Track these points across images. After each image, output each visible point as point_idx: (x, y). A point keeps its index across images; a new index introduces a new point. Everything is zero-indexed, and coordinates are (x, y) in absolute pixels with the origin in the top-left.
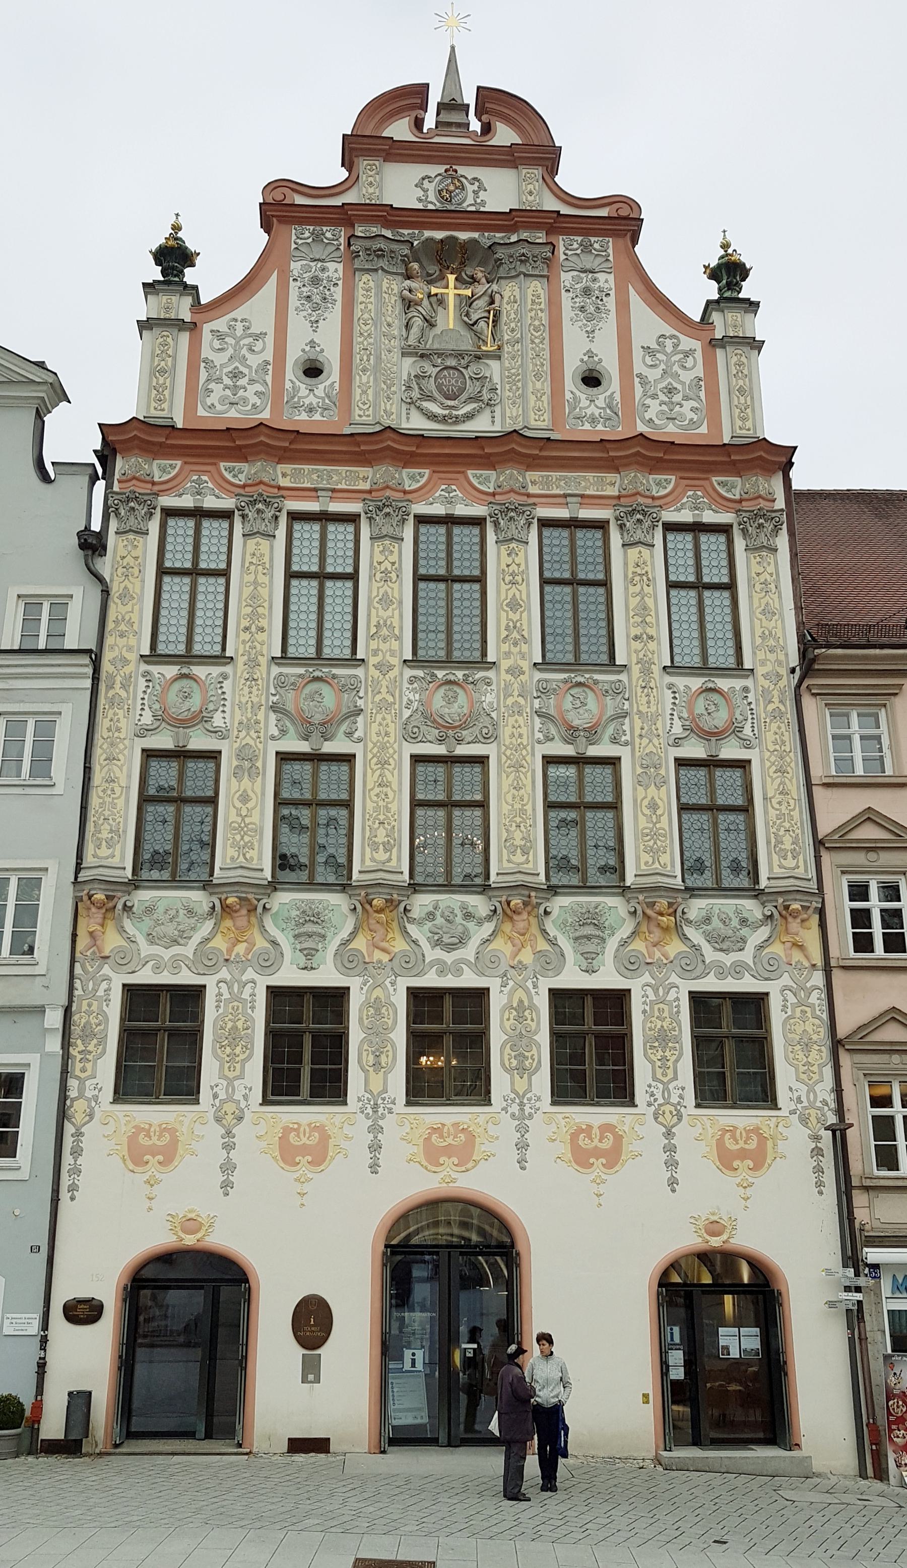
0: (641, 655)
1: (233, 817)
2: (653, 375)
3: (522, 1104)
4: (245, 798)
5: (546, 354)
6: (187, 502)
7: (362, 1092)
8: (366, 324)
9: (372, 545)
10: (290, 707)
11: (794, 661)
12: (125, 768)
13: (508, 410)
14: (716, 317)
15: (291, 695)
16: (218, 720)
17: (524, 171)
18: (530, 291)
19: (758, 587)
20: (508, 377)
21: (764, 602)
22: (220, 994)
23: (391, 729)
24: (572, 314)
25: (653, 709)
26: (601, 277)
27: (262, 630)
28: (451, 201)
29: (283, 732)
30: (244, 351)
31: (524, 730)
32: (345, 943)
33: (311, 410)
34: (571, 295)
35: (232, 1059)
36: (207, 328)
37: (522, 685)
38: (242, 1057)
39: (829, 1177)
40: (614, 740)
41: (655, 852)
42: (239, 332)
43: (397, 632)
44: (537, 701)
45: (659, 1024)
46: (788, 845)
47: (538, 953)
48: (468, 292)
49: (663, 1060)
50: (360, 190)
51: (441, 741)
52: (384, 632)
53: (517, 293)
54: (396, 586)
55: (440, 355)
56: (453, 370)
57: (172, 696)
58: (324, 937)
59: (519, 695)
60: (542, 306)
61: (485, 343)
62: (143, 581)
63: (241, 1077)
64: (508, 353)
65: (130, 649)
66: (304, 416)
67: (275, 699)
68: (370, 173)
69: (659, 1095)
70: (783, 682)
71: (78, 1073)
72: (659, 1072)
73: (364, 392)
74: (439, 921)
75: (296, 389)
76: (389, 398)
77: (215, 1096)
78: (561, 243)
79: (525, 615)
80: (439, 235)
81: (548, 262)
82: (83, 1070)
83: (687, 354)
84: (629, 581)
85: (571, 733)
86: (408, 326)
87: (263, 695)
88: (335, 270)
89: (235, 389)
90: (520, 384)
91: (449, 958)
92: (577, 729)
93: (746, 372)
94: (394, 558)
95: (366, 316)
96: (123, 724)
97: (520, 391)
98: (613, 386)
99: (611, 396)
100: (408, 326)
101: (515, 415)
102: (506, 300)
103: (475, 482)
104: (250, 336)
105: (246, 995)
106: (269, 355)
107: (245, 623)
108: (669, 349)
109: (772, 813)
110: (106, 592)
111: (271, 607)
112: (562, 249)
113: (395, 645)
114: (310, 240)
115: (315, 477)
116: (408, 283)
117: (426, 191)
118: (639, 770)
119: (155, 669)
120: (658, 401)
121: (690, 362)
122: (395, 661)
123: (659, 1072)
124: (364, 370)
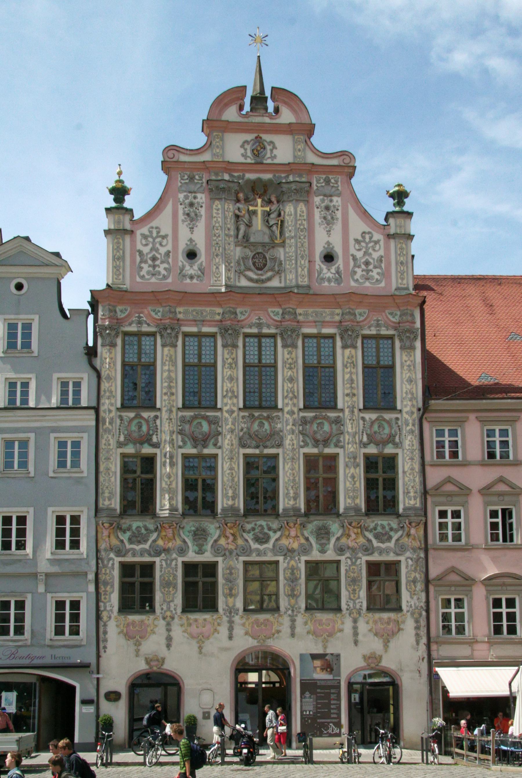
0: (349, 404)
1: (164, 485)
3: (293, 611)
5: (306, 245)
6: (133, 328)
7: (224, 607)
8: (217, 229)
9: (223, 350)
11: (420, 405)
12: (114, 463)
14: (391, 221)
15: (187, 427)
16: (155, 439)
17: (296, 137)
18: (298, 209)
19: (405, 368)
21: (408, 375)
22: (161, 565)
23: (234, 442)
24: (320, 221)
26: (335, 199)
27: (172, 394)
30: (158, 245)
31: (295, 442)
32: (216, 541)
33: (192, 277)
34: (319, 210)
36: (138, 233)
37: (294, 420)
38: (172, 592)
39: (424, 640)
40: (336, 446)
41: (354, 498)
42: (155, 235)
43: (236, 394)
45: (352, 575)
46: (412, 494)
47: (301, 545)
48: (268, 209)
50: (212, 151)
51: (257, 447)
52: (230, 394)
54: (235, 371)
55: (254, 246)
57: (134, 428)
58: (206, 539)
59: (293, 425)
61: (276, 239)
62: (116, 370)
63: (172, 601)
65: (112, 405)
66: (188, 281)
67: (180, 428)
68: (217, 140)
69: (351, 605)
70: (415, 415)
71: (103, 599)
74: (257, 531)
75: (184, 266)
77: (162, 609)
78: (315, 179)
81: (308, 192)
82: (105, 598)
83: (377, 242)
84: (345, 366)
85: (316, 443)
86: (238, 229)
88: (201, 198)
89: (154, 266)
90: (293, 262)
91: (262, 547)
92: (318, 441)
93: (404, 253)
94: (234, 356)
96: (111, 442)
97: (294, 266)
98: (340, 262)
99: (338, 268)
100: (238, 229)
103: (272, 315)
104: (160, 236)
106: (169, 247)
107: (165, 391)
108: (367, 240)
109: (407, 479)
110: (99, 376)
111: (176, 383)
113: (235, 401)
114: (187, 181)
115: (194, 313)
116: (238, 205)
117: (246, 150)
118: (347, 460)
119: (124, 414)
120: (361, 269)
122: (235, 409)
123: (352, 596)
124: (217, 255)
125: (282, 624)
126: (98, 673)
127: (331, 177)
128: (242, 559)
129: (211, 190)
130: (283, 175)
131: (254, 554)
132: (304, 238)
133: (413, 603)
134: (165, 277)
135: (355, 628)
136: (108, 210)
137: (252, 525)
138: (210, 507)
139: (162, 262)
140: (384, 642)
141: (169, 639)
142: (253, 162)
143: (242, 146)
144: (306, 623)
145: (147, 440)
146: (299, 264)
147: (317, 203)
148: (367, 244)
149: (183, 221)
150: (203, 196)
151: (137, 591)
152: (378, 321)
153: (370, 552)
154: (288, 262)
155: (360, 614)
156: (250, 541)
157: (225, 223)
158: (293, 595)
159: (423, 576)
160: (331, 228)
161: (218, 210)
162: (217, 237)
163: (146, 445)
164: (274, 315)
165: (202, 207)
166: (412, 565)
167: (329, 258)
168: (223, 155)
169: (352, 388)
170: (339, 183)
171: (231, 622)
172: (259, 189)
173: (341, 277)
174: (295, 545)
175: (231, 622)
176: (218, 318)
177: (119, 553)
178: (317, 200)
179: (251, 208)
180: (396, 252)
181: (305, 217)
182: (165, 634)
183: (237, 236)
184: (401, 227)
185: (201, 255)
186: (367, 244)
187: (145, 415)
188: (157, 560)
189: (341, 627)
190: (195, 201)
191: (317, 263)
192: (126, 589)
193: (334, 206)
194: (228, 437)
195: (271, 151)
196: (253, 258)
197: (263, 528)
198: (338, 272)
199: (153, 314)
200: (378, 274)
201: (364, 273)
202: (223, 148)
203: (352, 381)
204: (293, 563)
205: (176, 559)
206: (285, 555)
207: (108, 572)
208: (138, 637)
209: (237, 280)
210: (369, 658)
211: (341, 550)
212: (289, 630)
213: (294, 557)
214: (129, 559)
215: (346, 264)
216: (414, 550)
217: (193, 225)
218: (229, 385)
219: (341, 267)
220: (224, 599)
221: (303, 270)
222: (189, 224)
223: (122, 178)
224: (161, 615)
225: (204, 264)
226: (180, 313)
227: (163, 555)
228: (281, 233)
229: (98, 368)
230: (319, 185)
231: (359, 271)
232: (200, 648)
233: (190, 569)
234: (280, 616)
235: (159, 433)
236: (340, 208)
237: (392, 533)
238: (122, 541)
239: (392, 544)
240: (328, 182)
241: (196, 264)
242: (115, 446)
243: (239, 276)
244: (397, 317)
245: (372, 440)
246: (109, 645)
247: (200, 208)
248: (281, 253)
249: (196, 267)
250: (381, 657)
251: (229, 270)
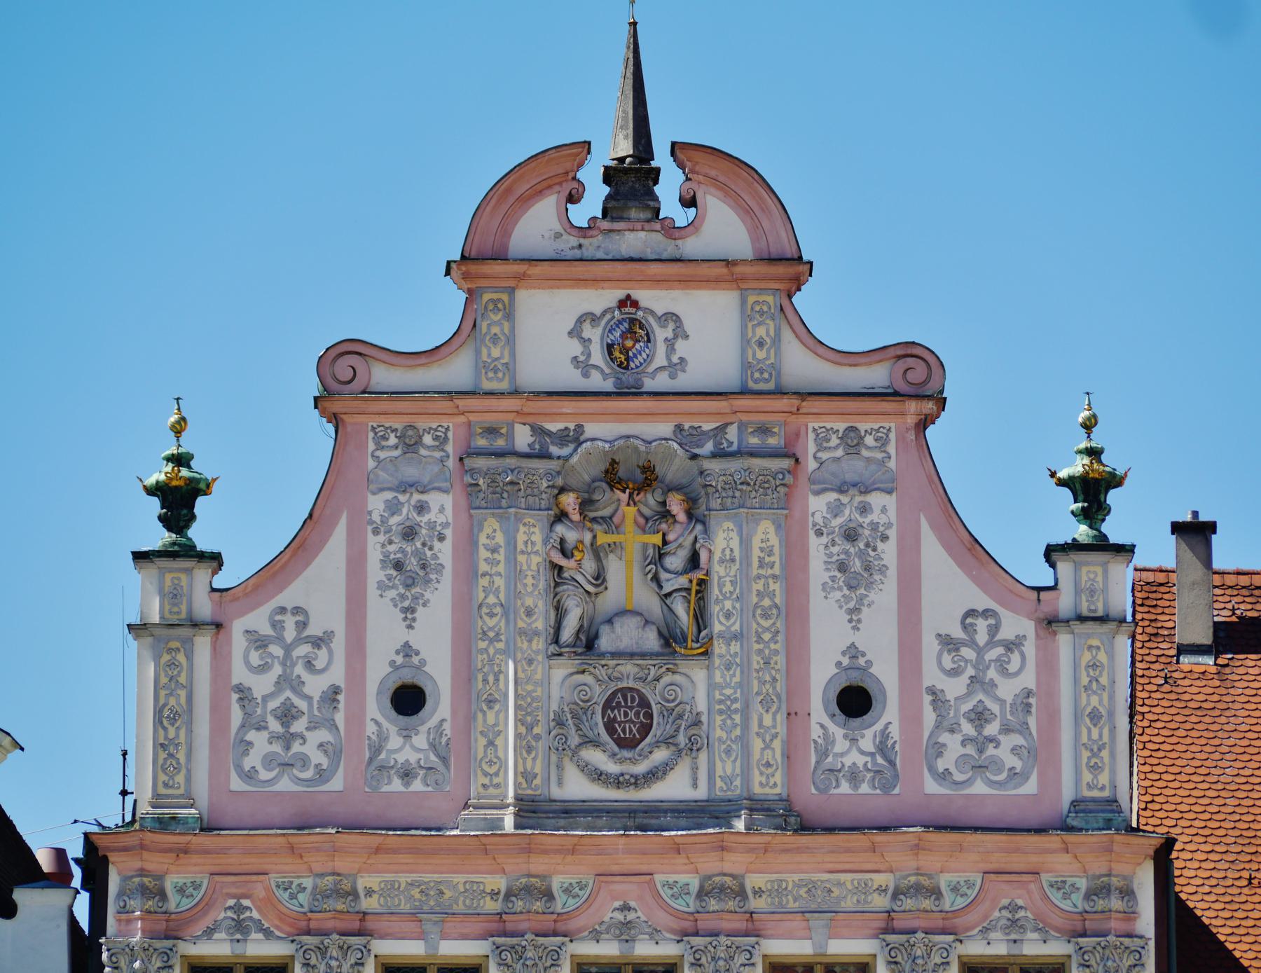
2: (954, 688)
5: (780, 661)
8: (491, 615)
13: (719, 765)
14: (1065, 567)
18: (756, 543)
20: (720, 702)
24: (825, 577)
26: (876, 499)
28: (627, 368)
30: (299, 670)
33: (407, 774)
34: (824, 540)
36: (238, 627)
42: (290, 634)
53: (735, 544)
60: (777, 570)
64: (721, 656)
66: (397, 785)
75: (383, 738)
83: (1010, 646)
88: (443, 507)
89: (287, 739)
90: (737, 718)
93: (1104, 680)
95: (491, 599)
97: (738, 732)
98: (889, 715)
99: (885, 734)
101: (729, 772)
103: (666, 893)
106: (337, 675)
108: (982, 638)
112: (812, 448)
114: (397, 453)
115: (416, 893)
116: (560, 529)
117: (586, 342)
121: (1016, 658)
127: (862, 427)
132: (773, 639)
134: (322, 775)
136: (139, 556)
142: (609, 386)
143: (575, 332)
146: (754, 727)
147: (818, 519)
148: (980, 651)
149: (382, 586)
150: (447, 500)
154: (719, 719)
157: (518, 595)
160: (861, 599)
162: (491, 641)
165: (441, 538)
167: (855, 701)
168: (510, 368)
170: (892, 449)
172: (631, 476)
173: (892, 763)
176: (491, 906)
178: (818, 505)
180: (1076, 680)
181: (777, 570)
184: (1092, 592)
185: (437, 703)
186: (980, 651)
191: (815, 719)
193: (874, 526)
195: (670, 345)
196: (608, 705)
198: (883, 747)
200: (1015, 750)
202: (511, 341)
209: (553, 778)
215: (911, 718)
217: (415, 598)
219: (895, 731)
222: (403, 597)
223: (188, 444)
225: (447, 727)
226: (369, 892)
228: (701, 618)
231: (953, 746)
236: (892, 533)
240: (852, 440)
241: (423, 729)
243: (560, 767)
244: (1078, 898)
247: (437, 545)
248: (696, 684)
249: (420, 741)
251: (529, 749)
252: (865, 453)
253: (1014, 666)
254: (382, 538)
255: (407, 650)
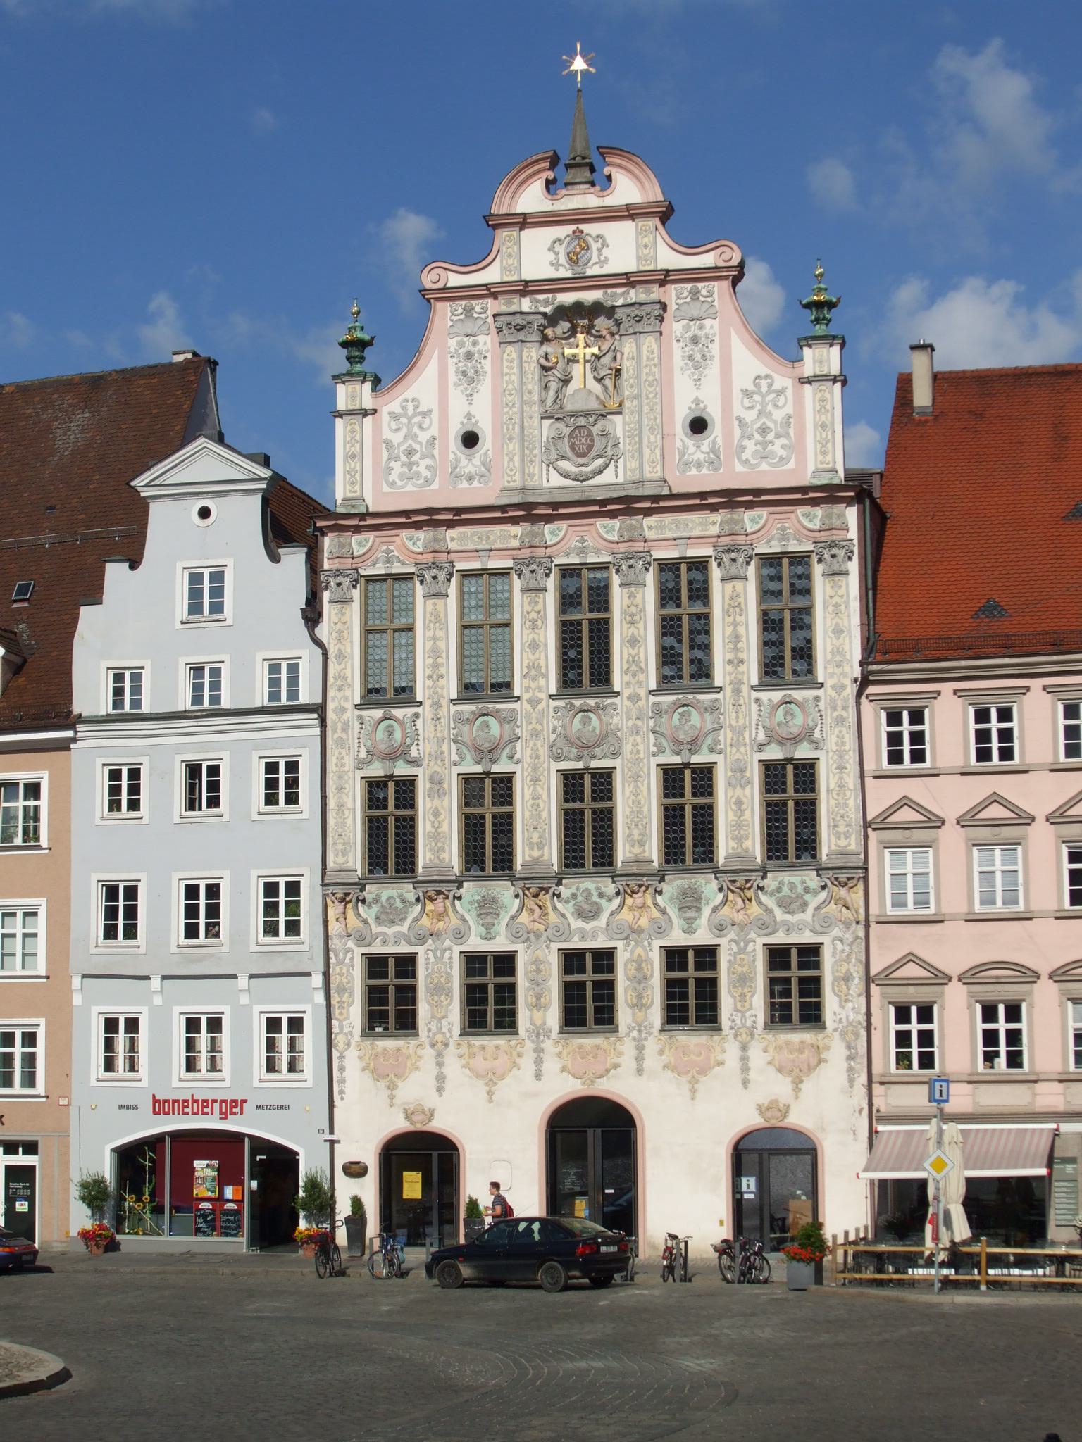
1: (429, 828)
2: (750, 416)
3: (639, 1031)
4: (436, 814)
5: (658, 407)
6: (379, 570)
7: (528, 1025)
10: (466, 739)
15: (466, 729)
16: (414, 753)
18: (645, 348)
24: (682, 363)
25: (741, 722)
26: (707, 322)
29: (462, 758)
30: (416, 429)
31: (641, 747)
32: (513, 918)
33: (470, 479)
34: (681, 344)
35: (440, 1006)
36: (384, 413)
37: (640, 709)
38: (446, 1003)
39: (863, 1078)
40: (711, 750)
41: (739, 839)
42: (410, 412)
43: (543, 670)
44: (652, 722)
45: (740, 969)
46: (842, 829)
49: (743, 994)
51: (579, 758)
52: (533, 672)
53: (634, 349)
56: (582, 434)
57: (381, 734)
65: (346, 699)
66: (465, 484)
69: (738, 1022)
72: (739, 1005)
73: (511, 460)
74: (580, 899)
75: (458, 461)
76: (531, 462)
77: (429, 1030)
78: (674, 292)
79: (642, 650)
80: (567, 298)
82: (341, 1014)
83: (781, 392)
84: (726, 612)
85: (678, 745)
87: (446, 730)
88: (487, 342)
89: (410, 465)
93: (828, 407)
98: (716, 431)
99: (714, 442)
102: (626, 356)
103: (602, 531)
104: (419, 414)
105: (446, 959)
106: (434, 431)
107: (428, 672)
108: (764, 389)
110: (325, 656)
112: (674, 298)
113: (542, 682)
114: (462, 317)
115: (476, 538)
116: (546, 348)
117: (557, 254)
118: (730, 774)
119: (365, 713)
120: (753, 442)
121: (782, 398)
122: (543, 696)
124: (510, 439)
125: (620, 1054)
126: (332, 1132)
128: (556, 946)
129: (499, 330)
130: (620, 290)
131: (576, 938)
133: (843, 1016)
135: (744, 1059)
137: (573, 890)
138: (504, 859)
139: (423, 457)
140: (793, 1082)
141: (441, 1078)
142: (569, 274)
143: (551, 249)
144: (661, 1052)
145: (400, 753)
146: (645, 442)
148: (763, 396)
150: (488, 339)
151: (390, 999)
152: (784, 529)
153: (769, 930)
155: (752, 1035)
156: (568, 915)
158: (639, 1004)
159: (862, 969)
160: (701, 374)
161: (511, 361)
163: (400, 763)
164: (607, 532)
165: (485, 357)
166: (843, 951)
167: (698, 426)
169: (736, 649)
170: (715, 296)
171: (539, 1051)
174: (644, 922)
175: (539, 1051)
176: (516, 543)
177: (361, 940)
179: (568, 351)
181: (656, 361)
182: (434, 1071)
183: (543, 402)
184: (821, 362)
186: (763, 396)
187: (398, 712)
188: (420, 950)
189: (720, 1057)
190: (474, 349)
192: (374, 997)
193: (707, 336)
194: (531, 744)
195: (600, 250)
196: (571, 436)
197: (590, 894)
198: (714, 450)
199: (409, 544)
201: (759, 448)
203: (736, 638)
204: (639, 950)
205: (450, 949)
206: (626, 938)
207: (344, 970)
208: (392, 1076)
209: (545, 476)
210: (768, 1109)
211: (720, 928)
212: (634, 1064)
213: (642, 942)
214: (377, 949)
215: (728, 434)
216: (847, 925)
217: (473, 389)
218: (531, 656)
219: (720, 441)
220: (528, 1013)
221: (653, 452)
224: (427, 1041)
226: (452, 539)
227: (430, 941)
229: (325, 641)
230: (680, 302)
231: (750, 445)
232: (490, 1093)
233: (474, 962)
234: (619, 1039)
235: (421, 742)
236: (716, 339)
237: (808, 897)
238: (365, 922)
239: (808, 915)
240: (695, 294)
241: (477, 455)
242: (352, 768)
245: (771, 737)
246: (348, 1088)
248: (617, 425)
250: (788, 1107)
252: (702, 299)
253: (781, 403)
254: (455, 360)
255: (469, 416)
